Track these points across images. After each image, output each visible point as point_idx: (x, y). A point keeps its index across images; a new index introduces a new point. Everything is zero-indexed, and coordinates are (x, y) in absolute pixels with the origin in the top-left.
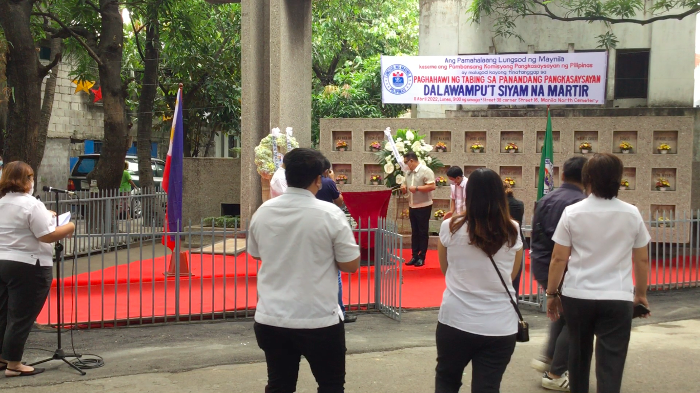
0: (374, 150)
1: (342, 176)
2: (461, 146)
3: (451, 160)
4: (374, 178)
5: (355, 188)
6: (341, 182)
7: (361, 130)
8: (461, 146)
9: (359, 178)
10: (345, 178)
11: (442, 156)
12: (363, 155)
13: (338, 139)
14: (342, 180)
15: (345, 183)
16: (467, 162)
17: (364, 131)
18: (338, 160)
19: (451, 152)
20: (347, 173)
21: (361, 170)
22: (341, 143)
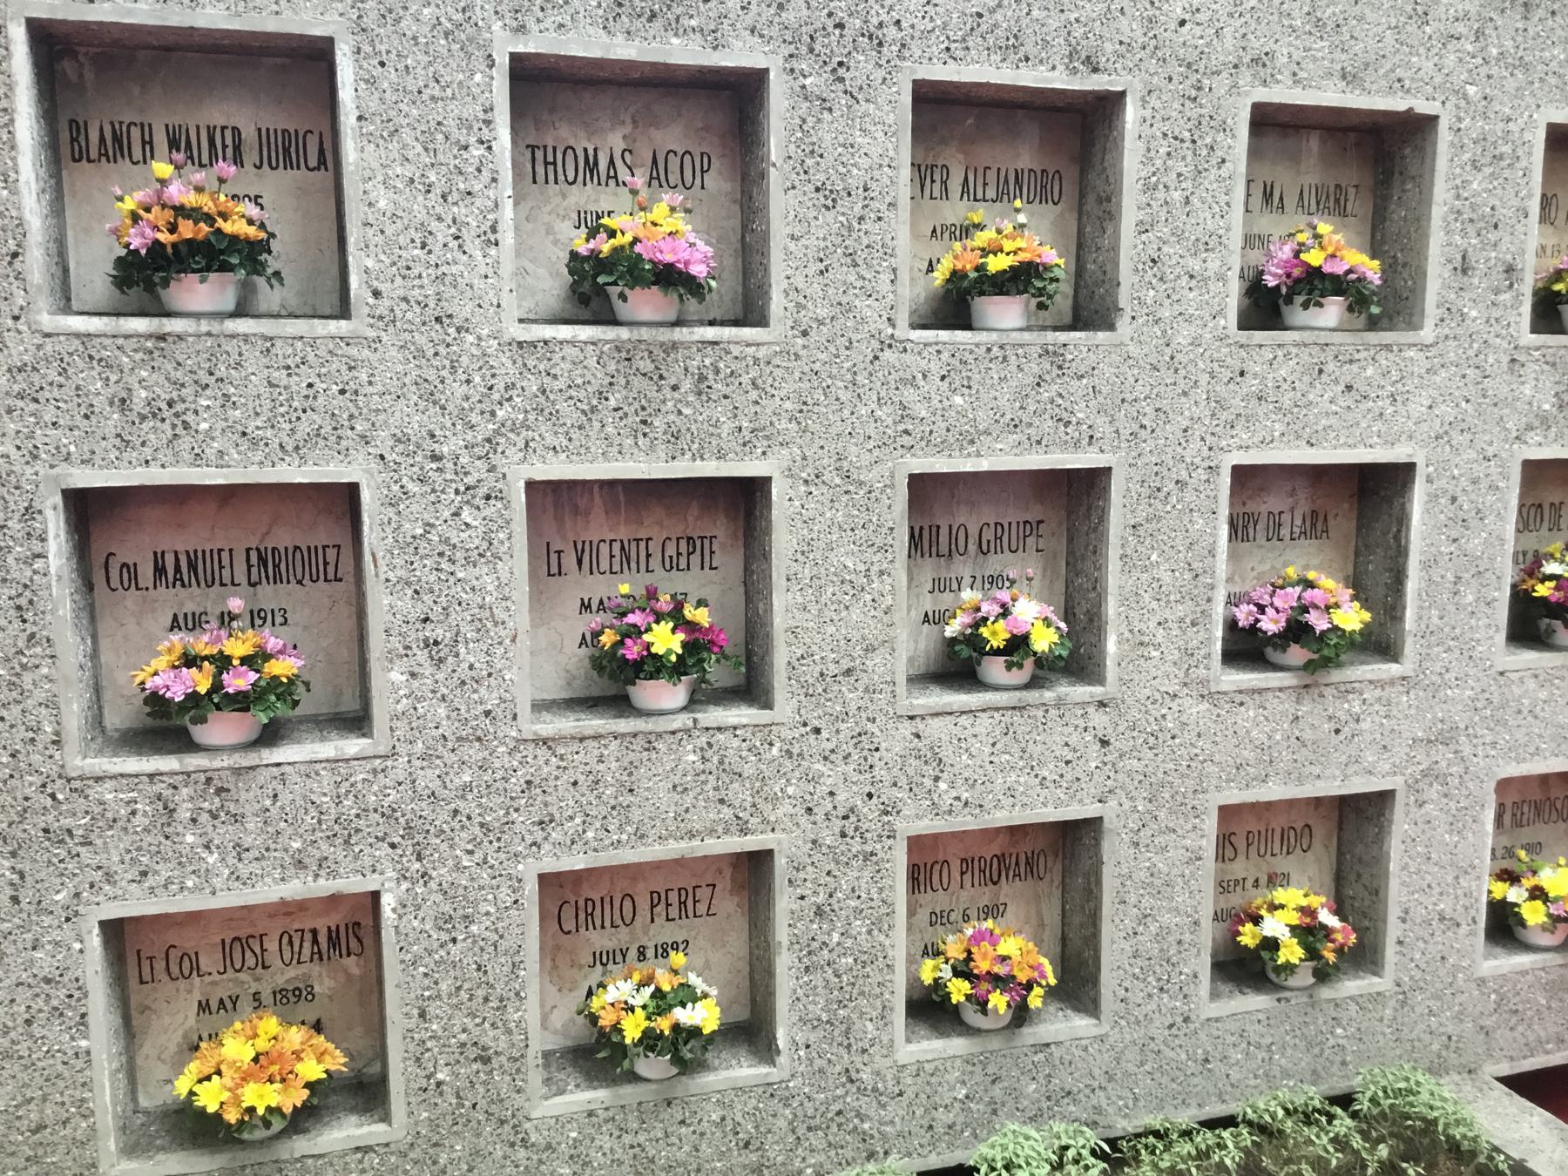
0: (645, 304)
1: (237, 648)
2: (1510, 269)
3: (1418, 408)
4: (665, 640)
5: (427, 779)
6: (221, 729)
7: (476, 48)
8: (1510, 269)
9: (471, 655)
10: (281, 667)
11: (1347, 373)
12: (506, 367)
13: (117, 147)
14: (241, 702)
15: (270, 735)
16: (1545, 422)
17: (504, 46)
18: (155, 434)
19: (1427, 333)
20: (269, 595)
21: (487, 554)
22: (179, 193)
